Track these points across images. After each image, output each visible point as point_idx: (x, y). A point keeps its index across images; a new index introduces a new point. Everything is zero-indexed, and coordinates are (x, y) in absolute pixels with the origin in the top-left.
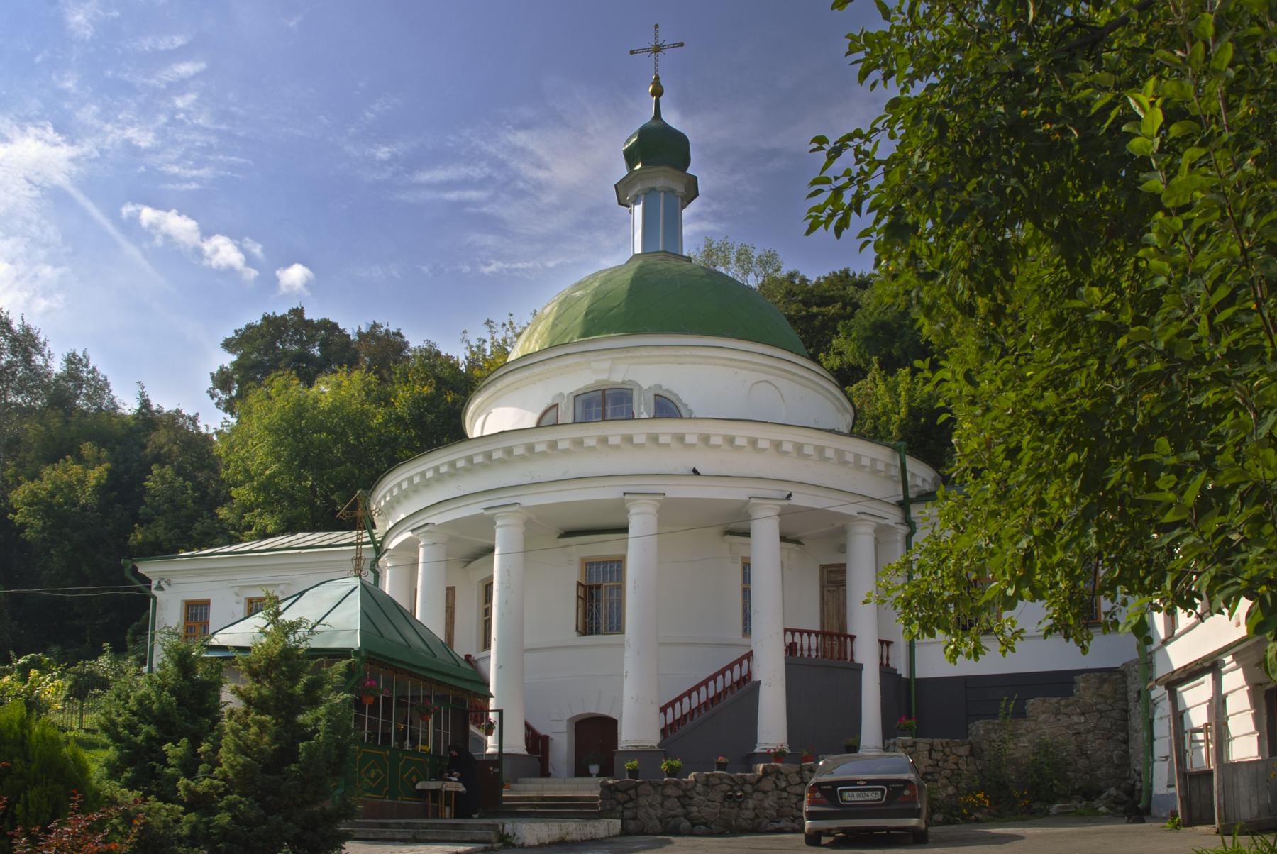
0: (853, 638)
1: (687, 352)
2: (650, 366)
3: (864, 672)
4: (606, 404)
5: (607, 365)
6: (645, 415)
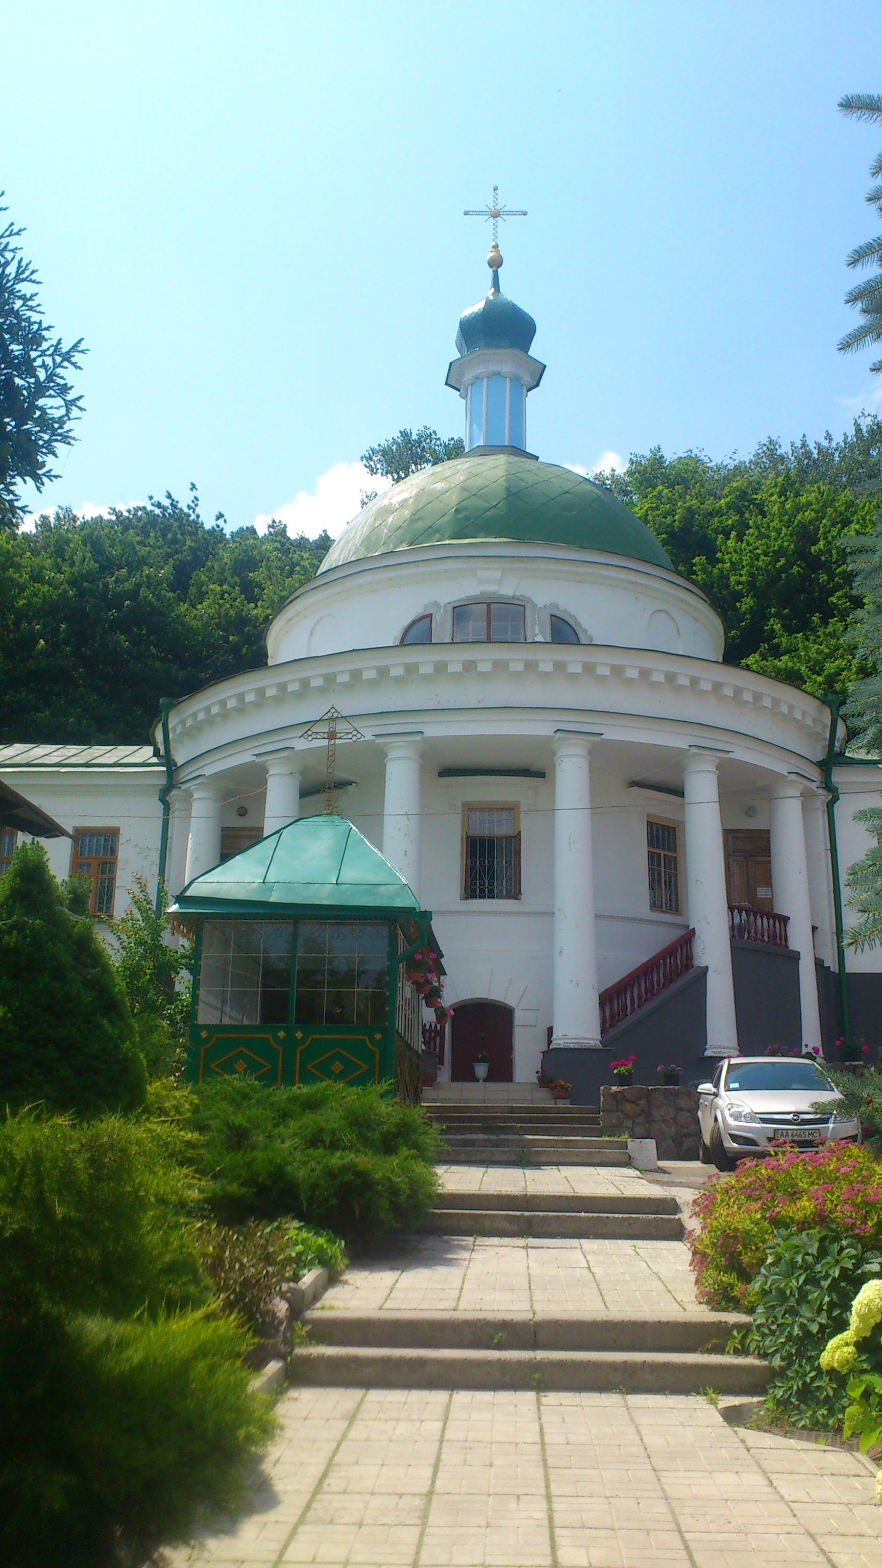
0: (785, 920)
1: (589, 569)
2: (549, 584)
3: (800, 961)
4: (493, 622)
5: (498, 574)
6: (539, 638)
